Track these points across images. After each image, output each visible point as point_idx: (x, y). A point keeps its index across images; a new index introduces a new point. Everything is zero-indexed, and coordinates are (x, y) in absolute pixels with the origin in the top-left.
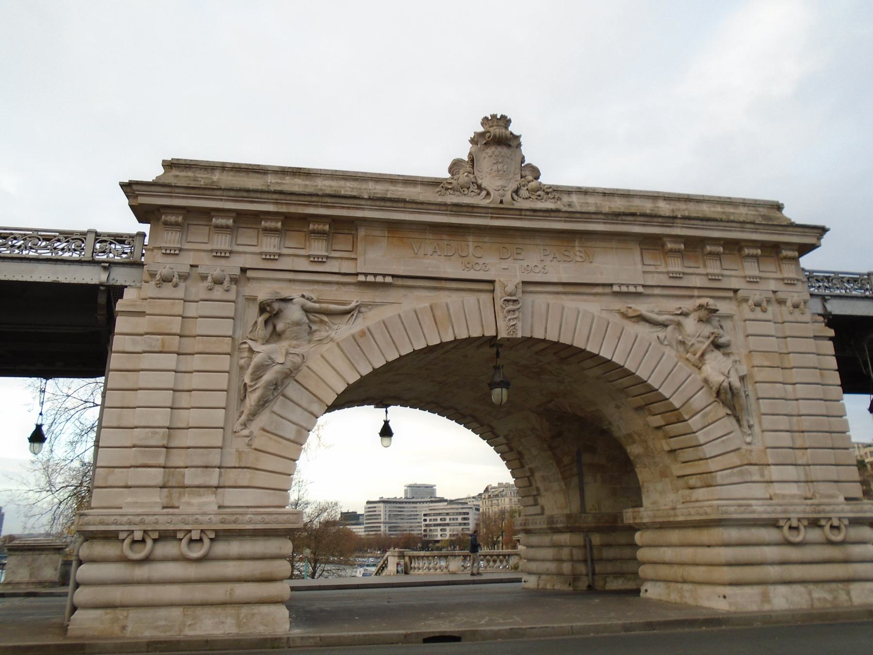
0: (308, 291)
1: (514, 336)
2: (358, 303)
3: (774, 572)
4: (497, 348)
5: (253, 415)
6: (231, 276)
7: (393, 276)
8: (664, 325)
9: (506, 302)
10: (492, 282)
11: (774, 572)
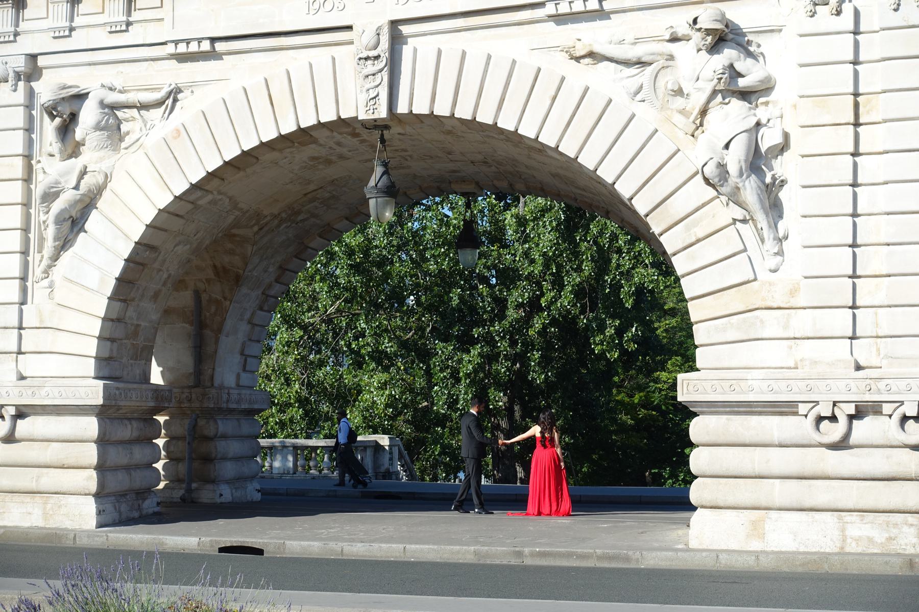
0: (110, 75)
1: (376, 116)
2: (172, 87)
3: (779, 492)
4: (382, 131)
5: (55, 258)
6: (17, 69)
7: (213, 40)
8: (641, 63)
9: (362, 61)
10: (349, 28)
11: (779, 492)
